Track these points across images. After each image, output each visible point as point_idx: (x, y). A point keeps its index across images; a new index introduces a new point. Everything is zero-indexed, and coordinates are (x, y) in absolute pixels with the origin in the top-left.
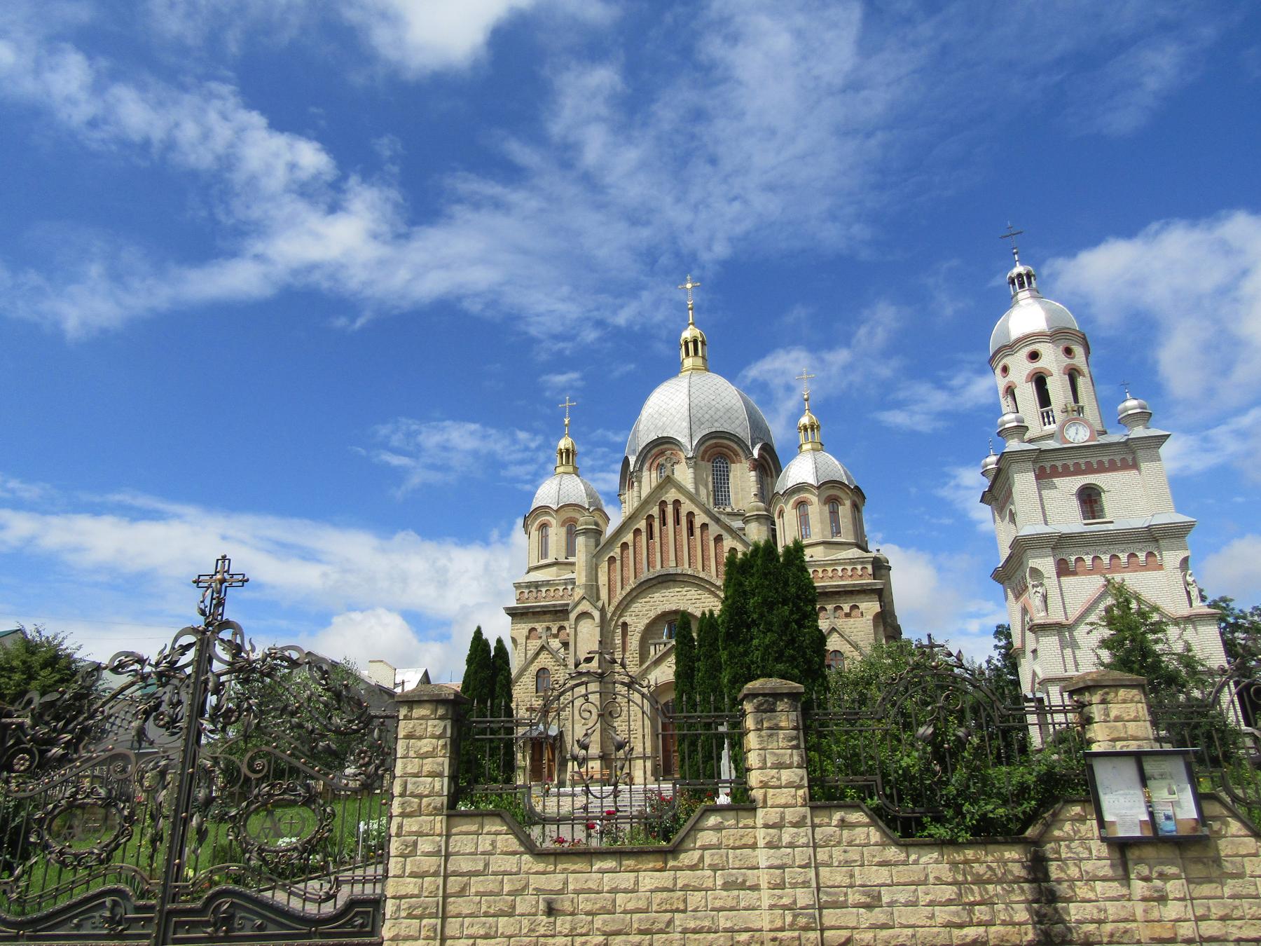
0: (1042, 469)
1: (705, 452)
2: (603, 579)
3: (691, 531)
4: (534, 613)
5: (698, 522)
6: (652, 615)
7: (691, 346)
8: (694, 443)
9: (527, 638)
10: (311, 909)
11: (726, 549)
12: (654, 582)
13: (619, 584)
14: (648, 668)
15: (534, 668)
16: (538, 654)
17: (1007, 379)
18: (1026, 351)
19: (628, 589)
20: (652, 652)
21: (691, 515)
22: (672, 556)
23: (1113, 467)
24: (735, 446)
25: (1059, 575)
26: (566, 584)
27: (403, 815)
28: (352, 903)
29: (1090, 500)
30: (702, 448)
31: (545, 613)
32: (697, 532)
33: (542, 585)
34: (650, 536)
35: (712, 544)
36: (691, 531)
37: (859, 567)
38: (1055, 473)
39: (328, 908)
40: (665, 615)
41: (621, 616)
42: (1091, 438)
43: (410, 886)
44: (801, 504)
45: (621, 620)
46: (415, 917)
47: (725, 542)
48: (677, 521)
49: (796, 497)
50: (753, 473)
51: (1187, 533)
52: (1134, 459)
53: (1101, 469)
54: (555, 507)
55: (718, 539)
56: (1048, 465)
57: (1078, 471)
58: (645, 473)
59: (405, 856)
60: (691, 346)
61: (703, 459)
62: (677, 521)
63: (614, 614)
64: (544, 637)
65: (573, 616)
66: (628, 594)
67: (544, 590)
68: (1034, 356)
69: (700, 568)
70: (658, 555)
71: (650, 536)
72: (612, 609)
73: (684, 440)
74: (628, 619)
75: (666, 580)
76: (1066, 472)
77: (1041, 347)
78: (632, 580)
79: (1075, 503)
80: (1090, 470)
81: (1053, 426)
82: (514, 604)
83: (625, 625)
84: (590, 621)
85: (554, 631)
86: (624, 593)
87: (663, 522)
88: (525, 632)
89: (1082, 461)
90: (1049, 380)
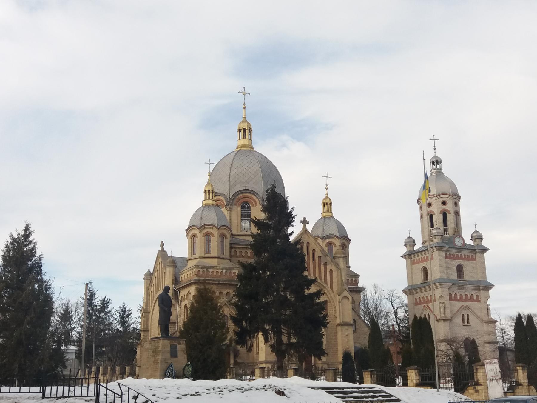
3: (314, 259)
5: (316, 256)
17: (429, 209)
21: (314, 250)
23: (468, 259)
26: (222, 269)
29: (460, 269)
33: (210, 268)
35: (322, 266)
36: (314, 259)
47: (328, 267)
49: (328, 240)
53: (465, 259)
55: (325, 264)
57: (457, 258)
79: (456, 271)
80: (461, 258)
89: (459, 254)
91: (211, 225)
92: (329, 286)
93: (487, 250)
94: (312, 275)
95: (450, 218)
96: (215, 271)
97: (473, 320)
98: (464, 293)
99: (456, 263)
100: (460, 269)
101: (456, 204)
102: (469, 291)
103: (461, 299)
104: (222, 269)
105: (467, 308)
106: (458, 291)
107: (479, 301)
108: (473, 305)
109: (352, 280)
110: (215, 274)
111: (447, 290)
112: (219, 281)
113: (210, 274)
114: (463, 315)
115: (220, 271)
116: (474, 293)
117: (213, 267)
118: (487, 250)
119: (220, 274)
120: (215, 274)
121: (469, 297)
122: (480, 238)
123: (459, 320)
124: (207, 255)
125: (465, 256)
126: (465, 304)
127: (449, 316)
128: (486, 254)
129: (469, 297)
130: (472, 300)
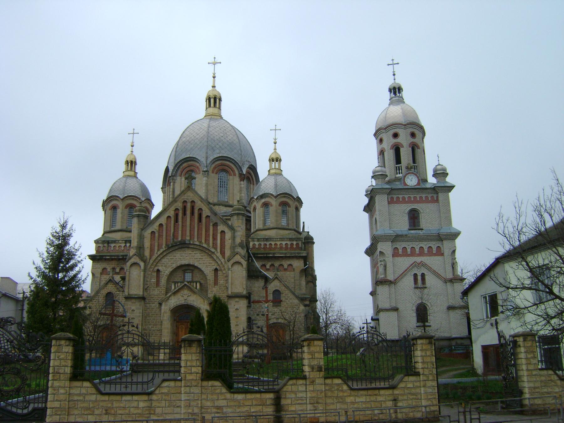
0: (392, 198)
1: (215, 168)
2: (147, 244)
3: (200, 220)
4: (106, 259)
5: (204, 216)
6: (174, 266)
7: (212, 101)
8: (208, 162)
9: (101, 274)
10: (20, 411)
11: (219, 231)
12: (177, 247)
13: (156, 248)
14: (170, 296)
15: (104, 292)
16: (107, 284)
18: (392, 132)
19: (161, 251)
20: (173, 287)
21: (200, 209)
22: (188, 233)
23: (427, 201)
24: (233, 166)
25: (393, 256)
27: (53, 380)
28: (34, 409)
29: (414, 217)
30: (213, 166)
31: (112, 259)
32: (204, 220)
33: (112, 243)
34: (176, 220)
36: (200, 220)
37: (295, 243)
38: (398, 201)
39: (25, 411)
40: (181, 266)
41: (156, 266)
42: (418, 184)
43: (57, 404)
44: (266, 205)
45: (156, 268)
46: (58, 415)
47: (219, 227)
48: (192, 213)
49: (263, 200)
50: (242, 182)
51: (456, 237)
52: (437, 197)
53: (421, 201)
54: (121, 197)
55: (215, 225)
56: (395, 197)
57: (410, 202)
58: (178, 178)
59: (54, 394)
60: (212, 101)
61: (213, 172)
62: (192, 213)
63: (152, 264)
64: (111, 275)
65: (129, 264)
66: (161, 254)
67: (113, 245)
68: (396, 135)
69: (203, 241)
70: (180, 232)
71: (176, 220)
72: (151, 262)
73: (203, 160)
74: (160, 268)
75: (183, 245)
76: (404, 201)
77: (400, 131)
78: (164, 246)
79: (406, 218)
80: (415, 201)
81: (401, 175)
82: (93, 252)
83: (158, 271)
84: (138, 268)
85: (118, 270)
86: (159, 253)
87: (184, 213)
88: (100, 270)
89: (412, 196)
90: (402, 150)
91: (117, 197)
92: (219, 250)
93: (451, 187)
94: (196, 239)
95: (405, 154)
96: (117, 245)
97: (430, 280)
98: (417, 246)
99: (408, 207)
100: (414, 217)
101: (413, 135)
102: (426, 243)
103: (413, 254)
104: (126, 243)
105: (422, 264)
106: (409, 243)
107: (442, 254)
108: (434, 262)
109: (292, 244)
110: (117, 249)
111: (389, 243)
112: (118, 256)
113: (112, 249)
114: (415, 275)
115: (123, 245)
116: (434, 245)
117: (114, 242)
118: (451, 187)
119: (123, 248)
120: (117, 249)
121: (426, 250)
122: (445, 174)
123: (408, 281)
124: (113, 229)
125: (421, 197)
126: (418, 259)
127: (391, 277)
128: (452, 194)
129: (426, 250)
130: (430, 253)
